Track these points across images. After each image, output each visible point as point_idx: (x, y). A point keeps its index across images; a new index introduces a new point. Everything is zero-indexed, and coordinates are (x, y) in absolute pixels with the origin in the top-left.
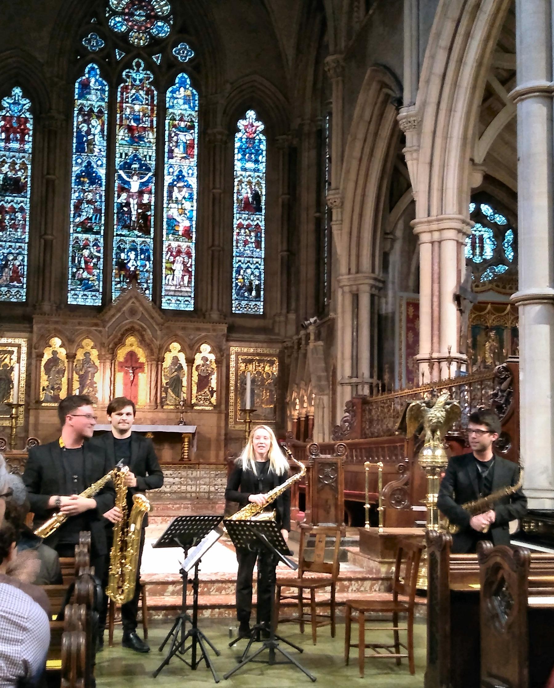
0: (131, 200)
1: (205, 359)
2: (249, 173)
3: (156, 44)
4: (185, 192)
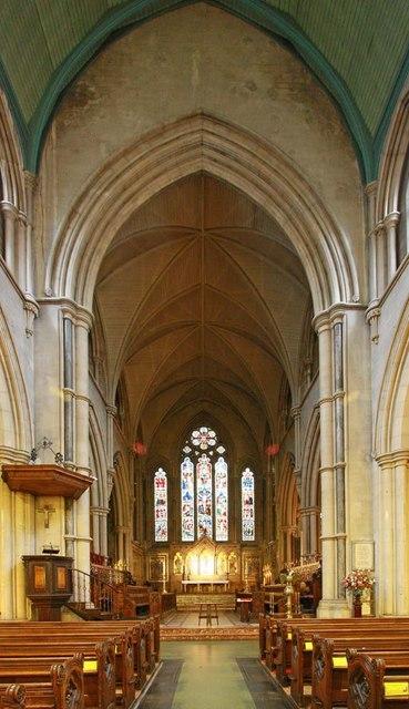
2: (248, 491)
3: (211, 448)
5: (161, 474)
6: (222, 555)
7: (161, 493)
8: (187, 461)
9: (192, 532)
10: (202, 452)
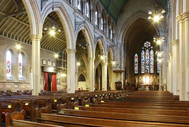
5: (136, 55)
6: (152, 77)
7: (136, 60)
8: (143, 51)
9: (144, 71)
10: (147, 48)
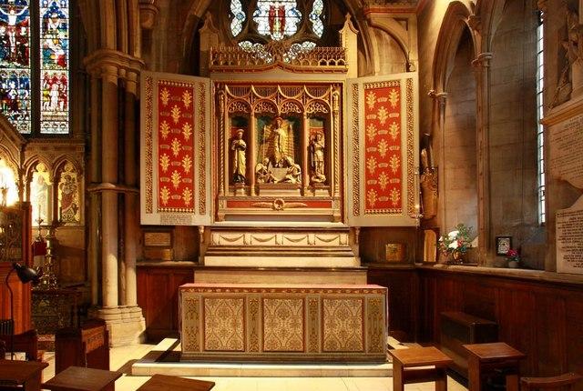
0: (10, 34)
1: (69, 178)
4: (59, 22)
